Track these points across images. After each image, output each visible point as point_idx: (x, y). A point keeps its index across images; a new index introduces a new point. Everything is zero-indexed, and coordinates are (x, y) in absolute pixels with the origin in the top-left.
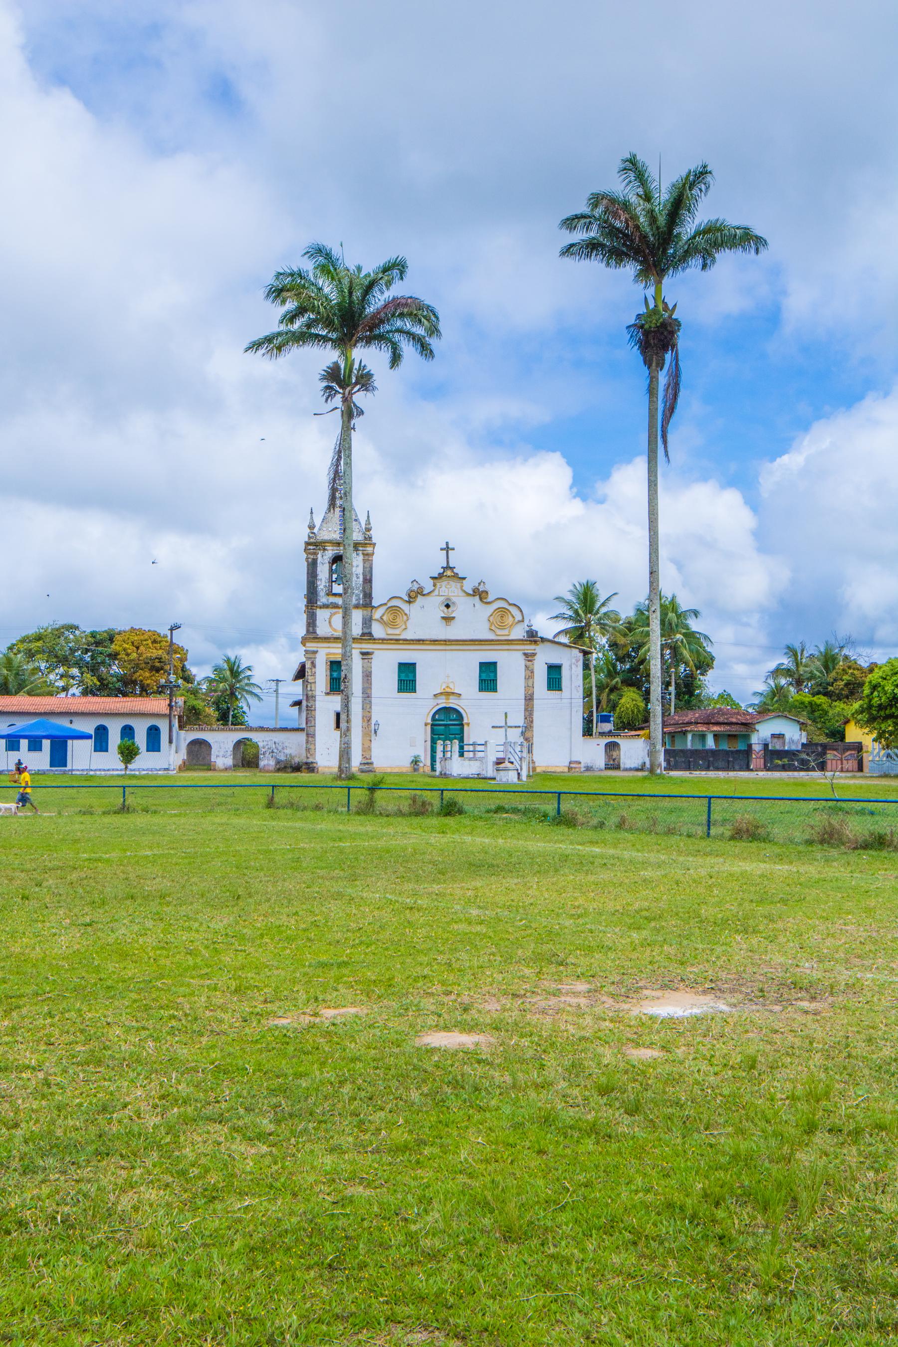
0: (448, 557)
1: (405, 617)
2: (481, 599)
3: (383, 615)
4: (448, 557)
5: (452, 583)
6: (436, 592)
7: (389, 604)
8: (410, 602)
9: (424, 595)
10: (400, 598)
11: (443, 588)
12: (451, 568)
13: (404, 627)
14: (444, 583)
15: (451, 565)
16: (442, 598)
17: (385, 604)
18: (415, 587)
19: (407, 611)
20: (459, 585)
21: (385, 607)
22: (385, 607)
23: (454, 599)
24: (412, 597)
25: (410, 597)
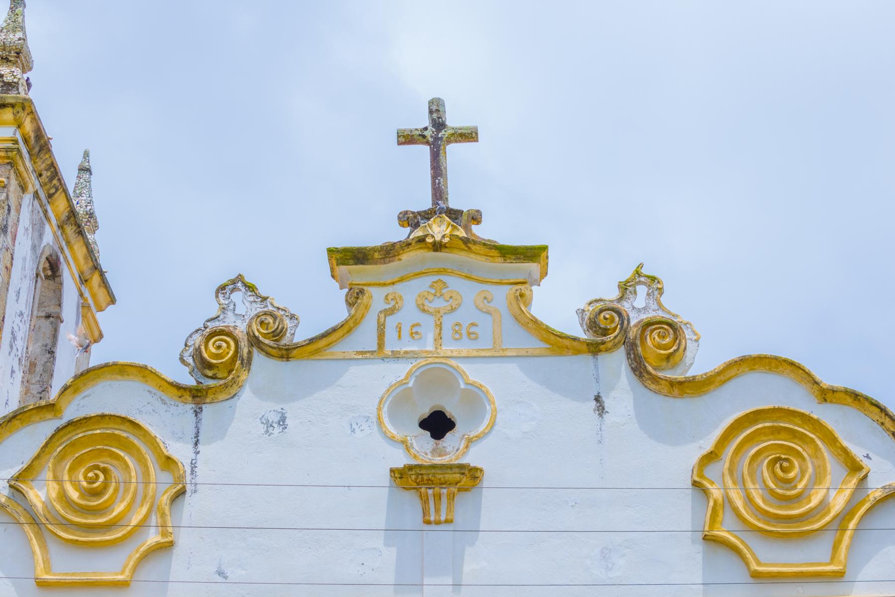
0: (437, 169)
1: (162, 483)
2: (639, 368)
3: (27, 473)
4: (437, 169)
5: (455, 283)
6: (365, 337)
7: (72, 411)
8: (198, 396)
9: (286, 353)
10: (143, 372)
11: (408, 314)
12: (454, 215)
13: (153, 537)
14: (411, 292)
15: (454, 203)
16: (399, 371)
17: (51, 407)
18: (241, 314)
19: (180, 451)
20: (501, 295)
21: (46, 428)
22: (46, 428)
23: (474, 373)
24: (211, 376)
25: (203, 365)
